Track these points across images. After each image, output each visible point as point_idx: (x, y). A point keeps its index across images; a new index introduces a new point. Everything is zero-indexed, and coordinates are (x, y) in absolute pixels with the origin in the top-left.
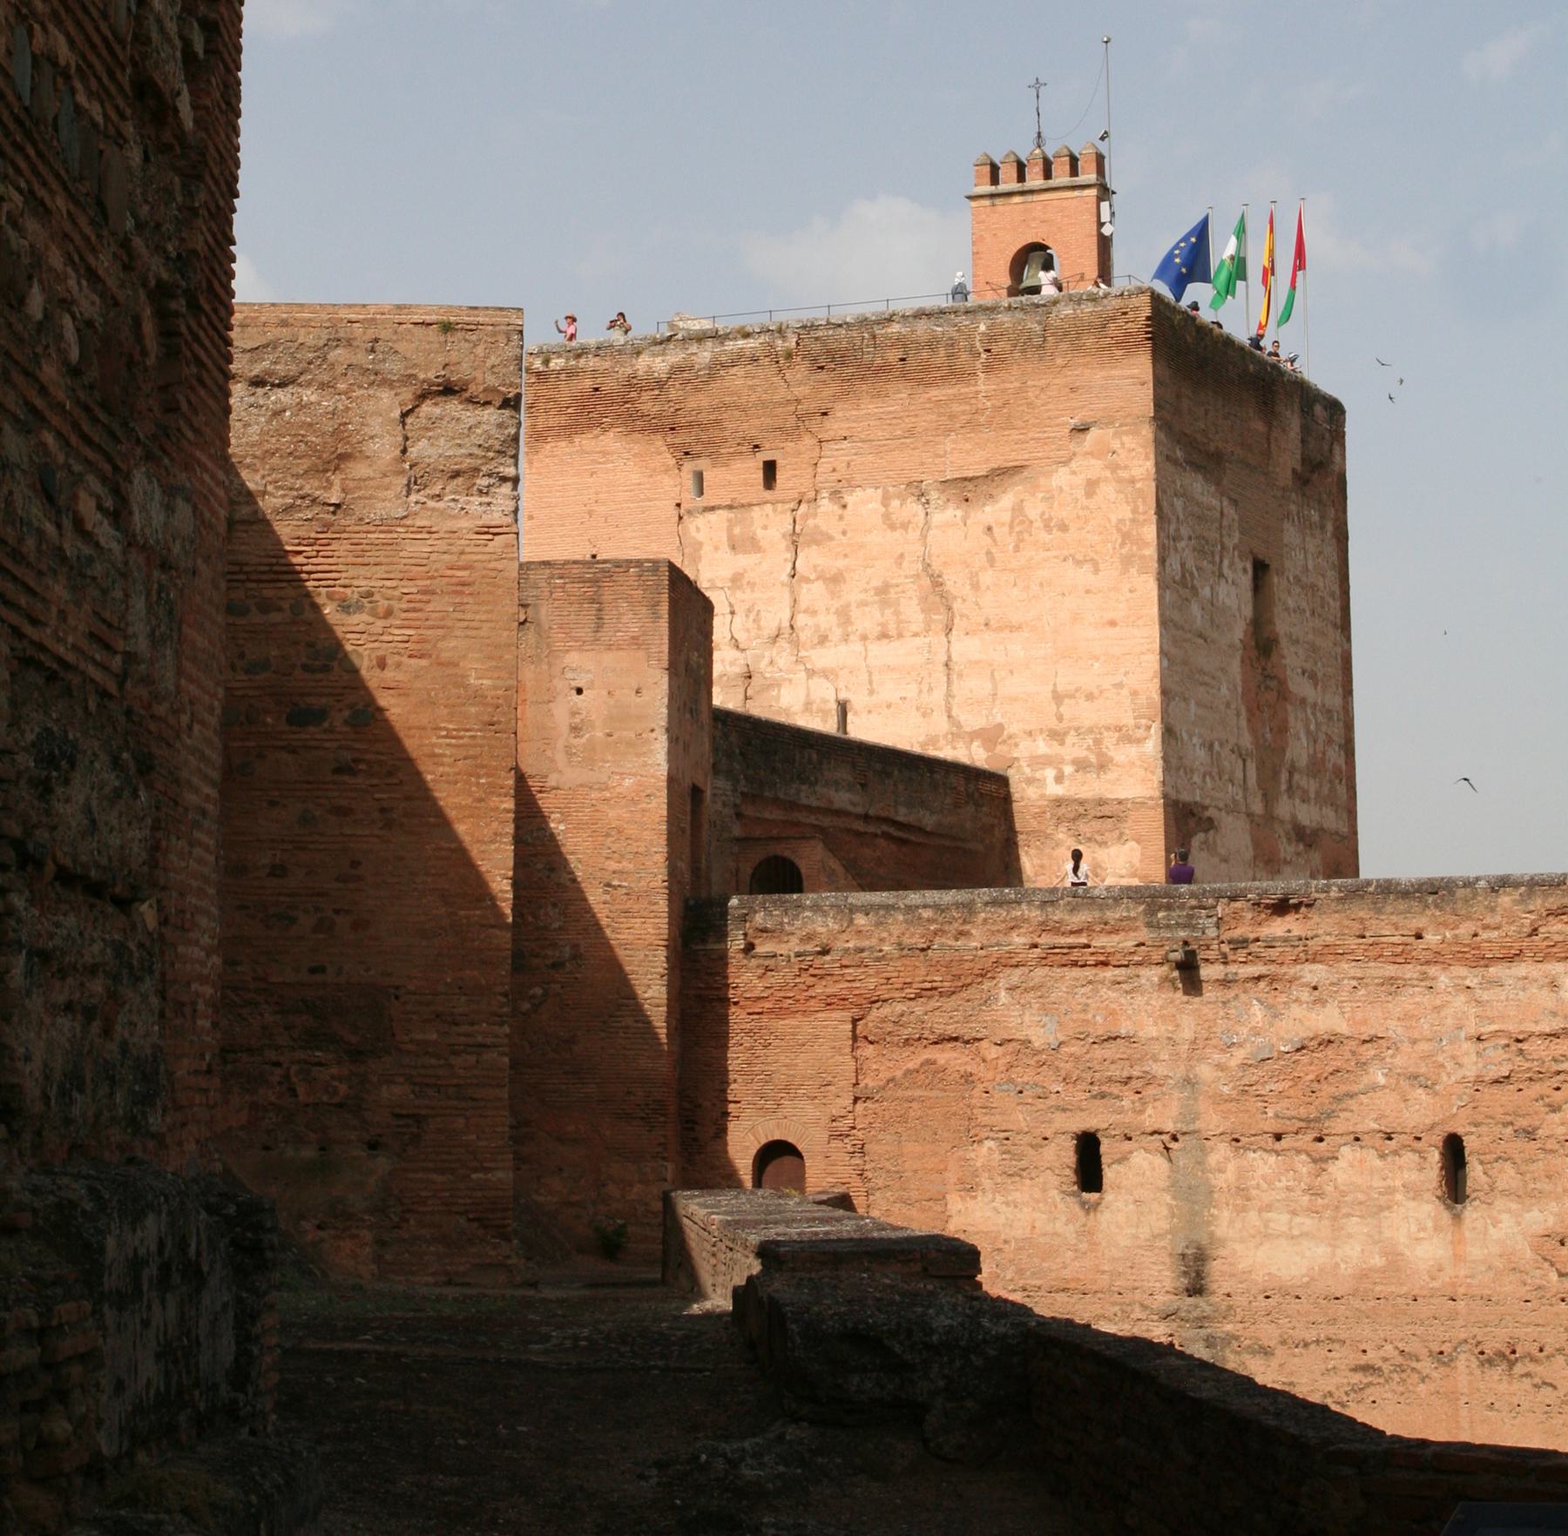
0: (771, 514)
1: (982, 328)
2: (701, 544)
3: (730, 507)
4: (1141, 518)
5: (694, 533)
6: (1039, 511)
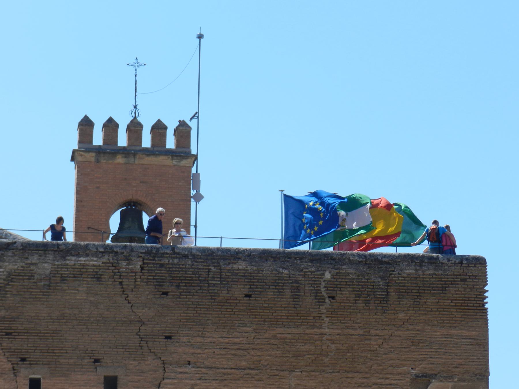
1: (328, 276)
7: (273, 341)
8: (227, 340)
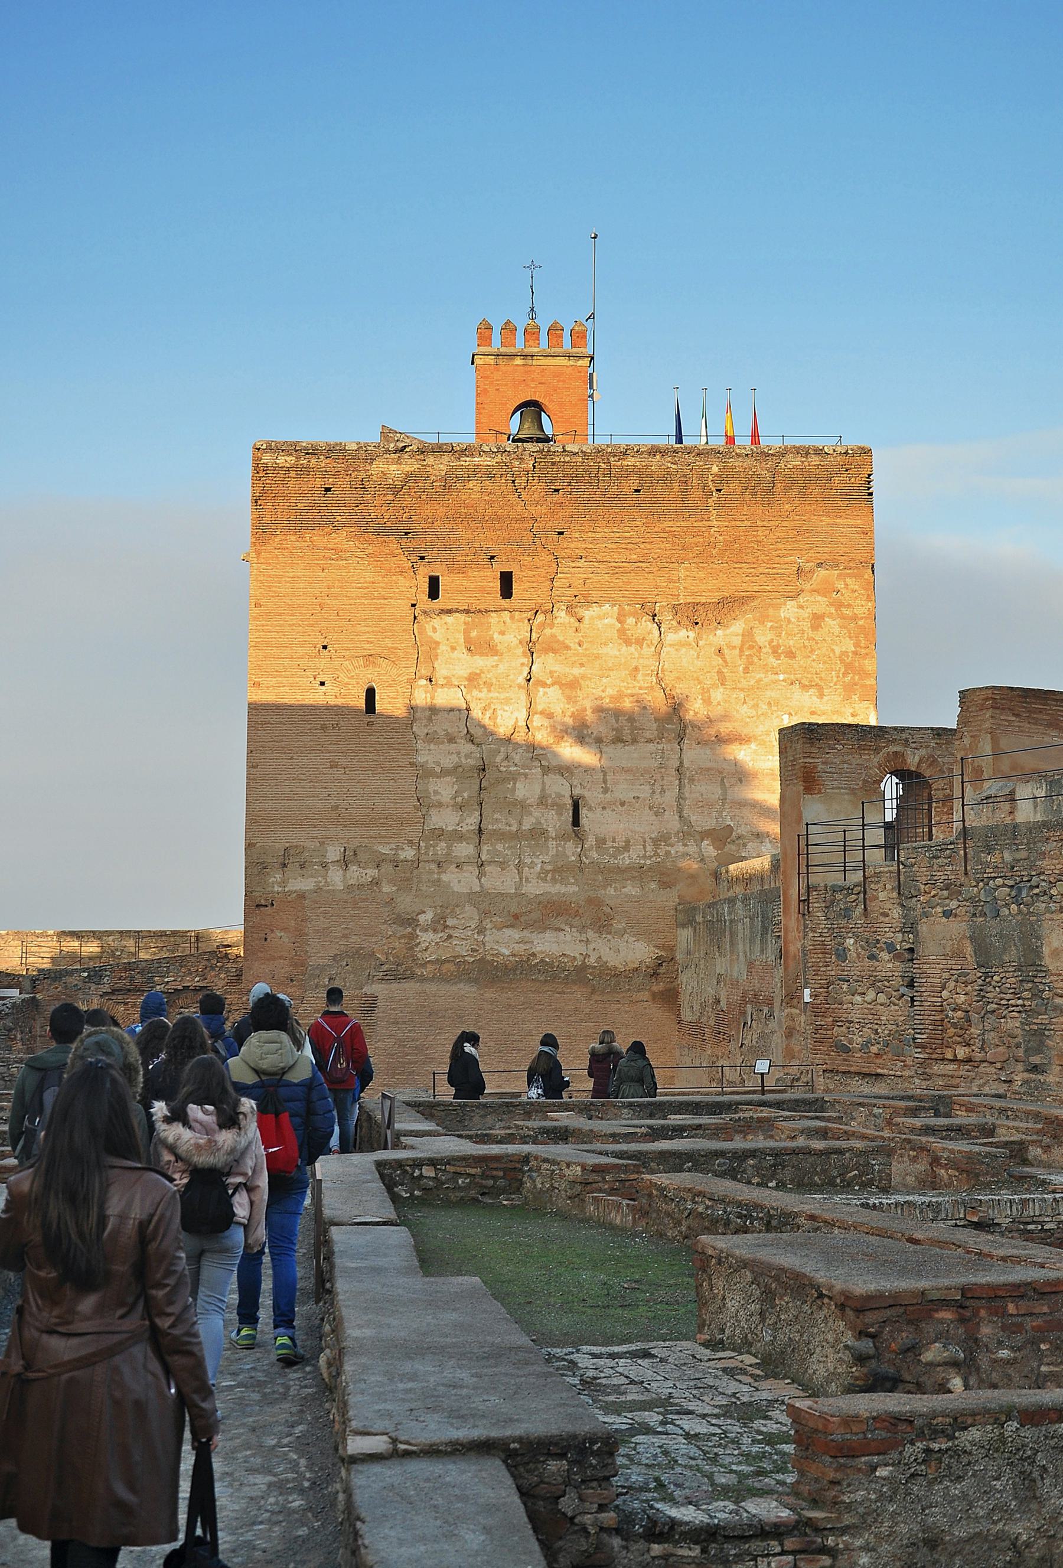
0: (508, 620)
1: (715, 469)
2: (438, 643)
3: (467, 612)
4: (863, 651)
5: (430, 633)
6: (769, 638)
7: (662, 535)
8: (618, 535)
